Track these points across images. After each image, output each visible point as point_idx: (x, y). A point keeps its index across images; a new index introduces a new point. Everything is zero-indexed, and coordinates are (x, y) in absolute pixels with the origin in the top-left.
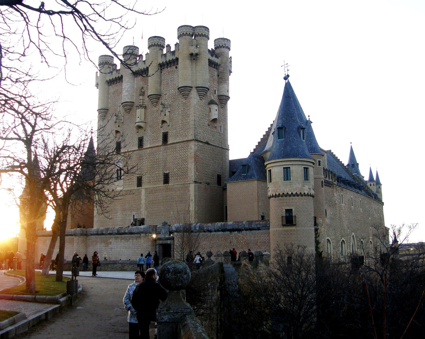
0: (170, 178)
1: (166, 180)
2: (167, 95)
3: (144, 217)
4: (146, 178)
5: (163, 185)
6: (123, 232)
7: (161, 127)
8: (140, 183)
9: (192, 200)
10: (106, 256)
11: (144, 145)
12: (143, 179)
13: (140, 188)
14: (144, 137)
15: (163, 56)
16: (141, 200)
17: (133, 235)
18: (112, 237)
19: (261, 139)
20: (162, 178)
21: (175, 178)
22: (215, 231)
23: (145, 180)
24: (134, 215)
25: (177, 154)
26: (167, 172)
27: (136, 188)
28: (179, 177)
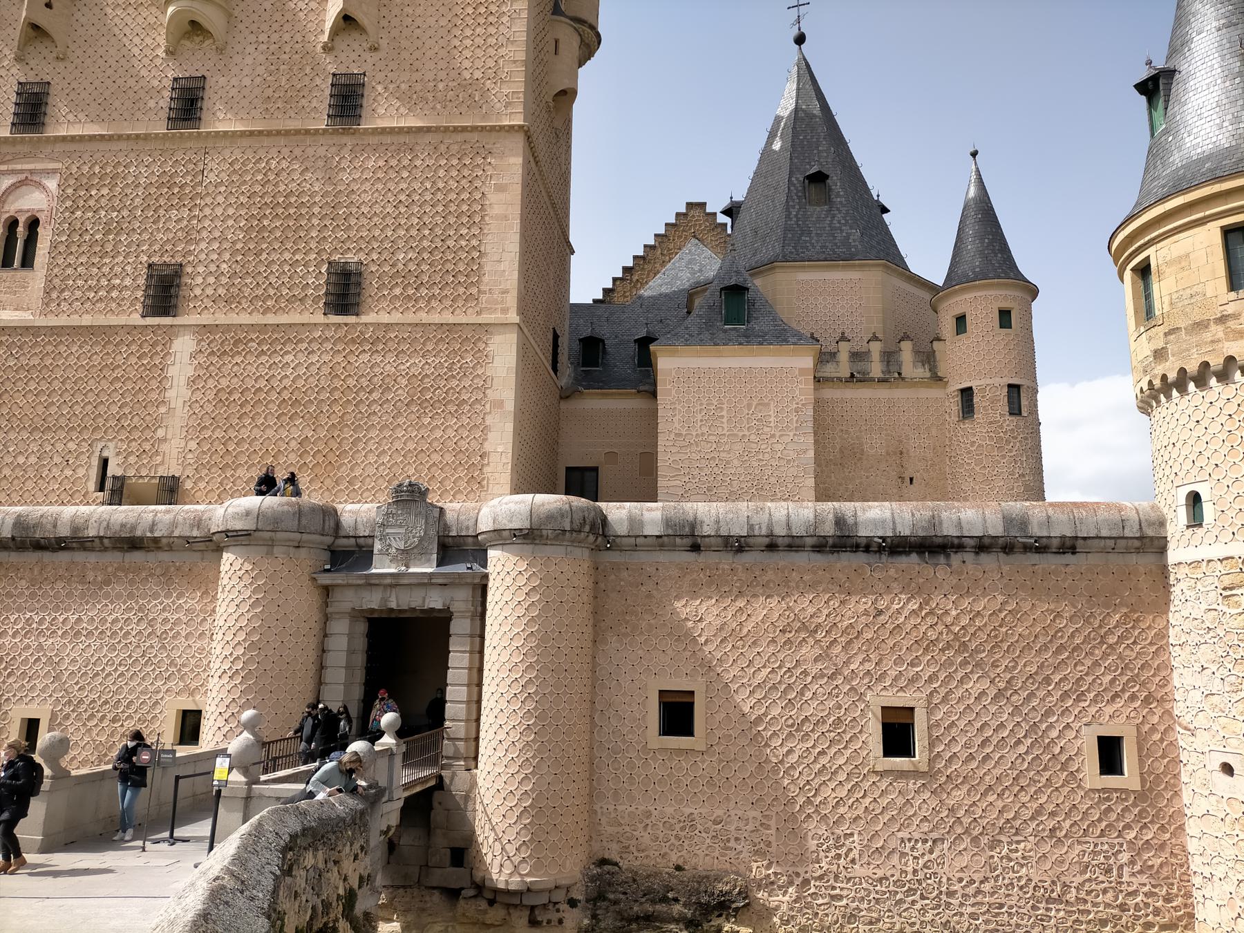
1: (345, 292)
3: (175, 471)
5: (319, 318)
6: (64, 532)
7: (327, 48)
8: (165, 292)
9: (499, 404)
11: (205, 115)
17: (137, 557)
19: (635, 257)
20: (317, 282)
21: (397, 291)
22: (772, 547)
23: (197, 283)
25: (416, 185)
26: (352, 258)
27: (136, 319)
28: (424, 291)
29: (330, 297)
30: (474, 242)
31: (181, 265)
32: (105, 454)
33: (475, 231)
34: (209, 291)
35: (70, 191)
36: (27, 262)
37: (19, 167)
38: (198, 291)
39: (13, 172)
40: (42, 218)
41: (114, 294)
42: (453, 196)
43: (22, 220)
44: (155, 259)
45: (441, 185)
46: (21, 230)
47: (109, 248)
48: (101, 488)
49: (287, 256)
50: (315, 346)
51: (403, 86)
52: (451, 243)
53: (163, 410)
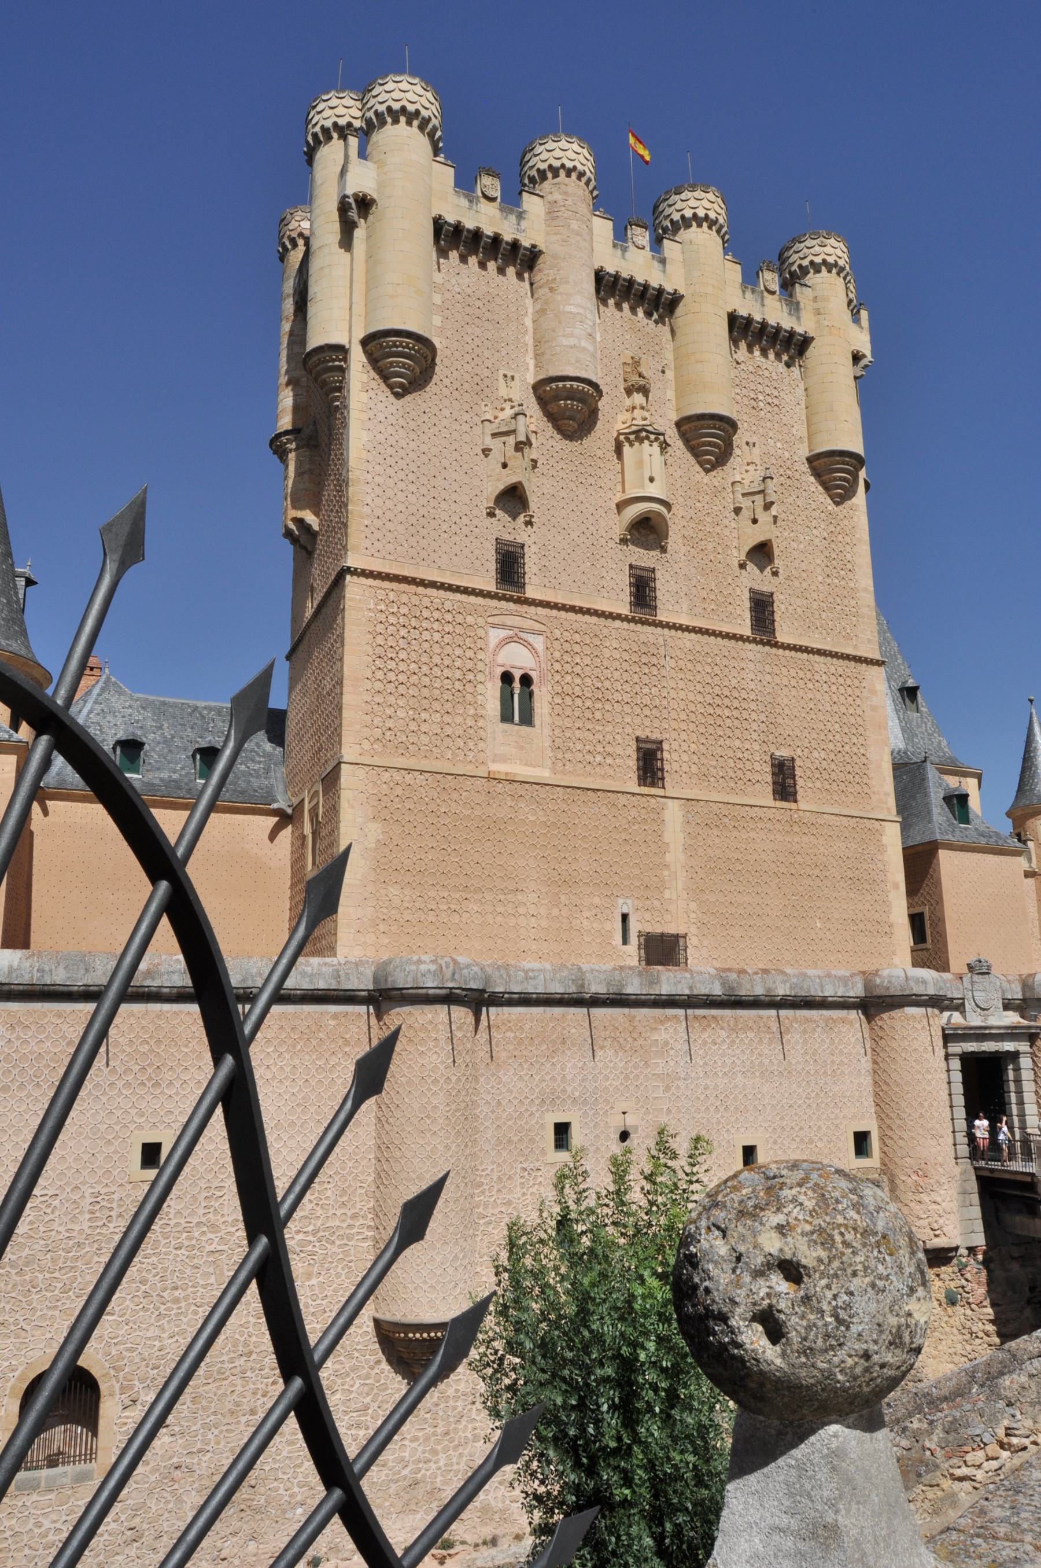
0: (800, 782)
1: (784, 781)
2: (756, 451)
4: (685, 757)
6: (759, 990)
8: (650, 764)
9: (896, 886)
10: (631, 1121)
12: (666, 755)
13: (659, 792)
14: (658, 574)
15: (748, 294)
16: (663, 849)
18: (668, 1019)
21: (818, 784)
24: (625, 917)
26: (783, 753)
29: (792, 790)
30: (862, 751)
31: (661, 742)
32: (625, 911)
33: (861, 740)
34: (685, 768)
35: (557, 655)
36: (527, 719)
37: (510, 620)
38: (675, 766)
39: (503, 626)
40: (534, 675)
41: (609, 760)
42: (843, 709)
43: (517, 674)
44: (639, 733)
45: (835, 699)
46: (517, 684)
47: (598, 715)
48: (625, 941)
49: (738, 743)
50: (769, 825)
51: (799, 610)
52: (847, 748)
53: (666, 873)
